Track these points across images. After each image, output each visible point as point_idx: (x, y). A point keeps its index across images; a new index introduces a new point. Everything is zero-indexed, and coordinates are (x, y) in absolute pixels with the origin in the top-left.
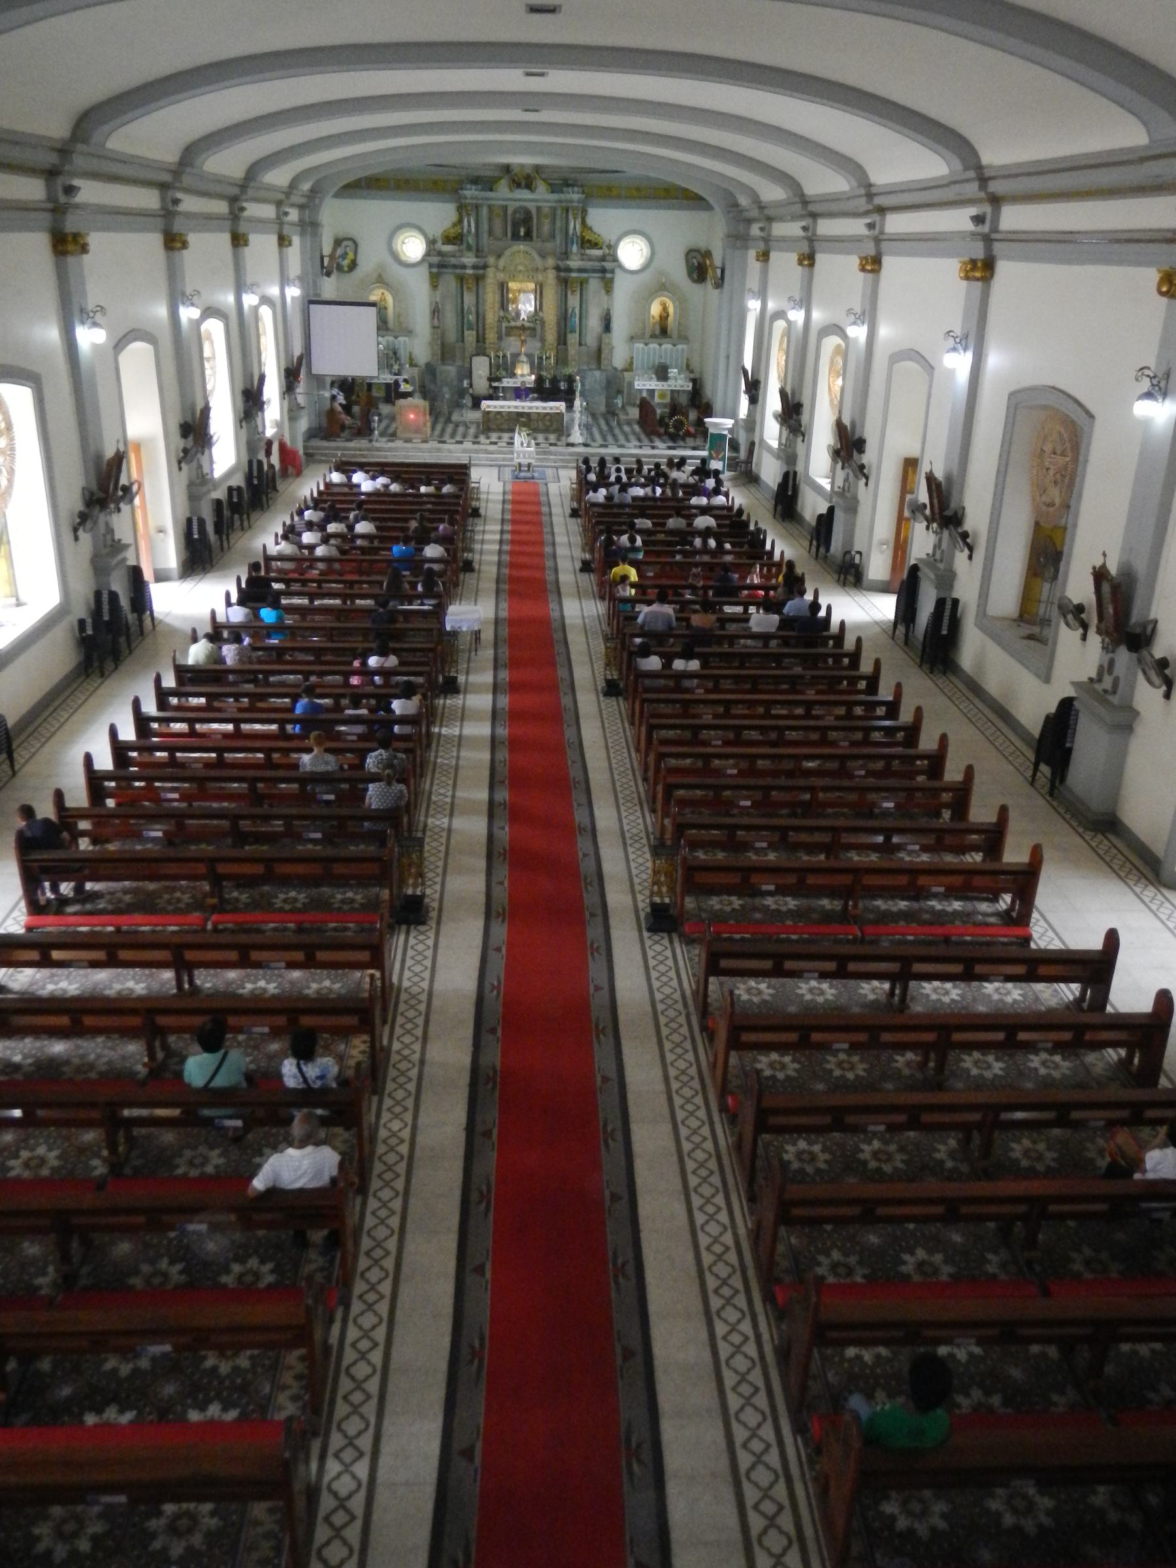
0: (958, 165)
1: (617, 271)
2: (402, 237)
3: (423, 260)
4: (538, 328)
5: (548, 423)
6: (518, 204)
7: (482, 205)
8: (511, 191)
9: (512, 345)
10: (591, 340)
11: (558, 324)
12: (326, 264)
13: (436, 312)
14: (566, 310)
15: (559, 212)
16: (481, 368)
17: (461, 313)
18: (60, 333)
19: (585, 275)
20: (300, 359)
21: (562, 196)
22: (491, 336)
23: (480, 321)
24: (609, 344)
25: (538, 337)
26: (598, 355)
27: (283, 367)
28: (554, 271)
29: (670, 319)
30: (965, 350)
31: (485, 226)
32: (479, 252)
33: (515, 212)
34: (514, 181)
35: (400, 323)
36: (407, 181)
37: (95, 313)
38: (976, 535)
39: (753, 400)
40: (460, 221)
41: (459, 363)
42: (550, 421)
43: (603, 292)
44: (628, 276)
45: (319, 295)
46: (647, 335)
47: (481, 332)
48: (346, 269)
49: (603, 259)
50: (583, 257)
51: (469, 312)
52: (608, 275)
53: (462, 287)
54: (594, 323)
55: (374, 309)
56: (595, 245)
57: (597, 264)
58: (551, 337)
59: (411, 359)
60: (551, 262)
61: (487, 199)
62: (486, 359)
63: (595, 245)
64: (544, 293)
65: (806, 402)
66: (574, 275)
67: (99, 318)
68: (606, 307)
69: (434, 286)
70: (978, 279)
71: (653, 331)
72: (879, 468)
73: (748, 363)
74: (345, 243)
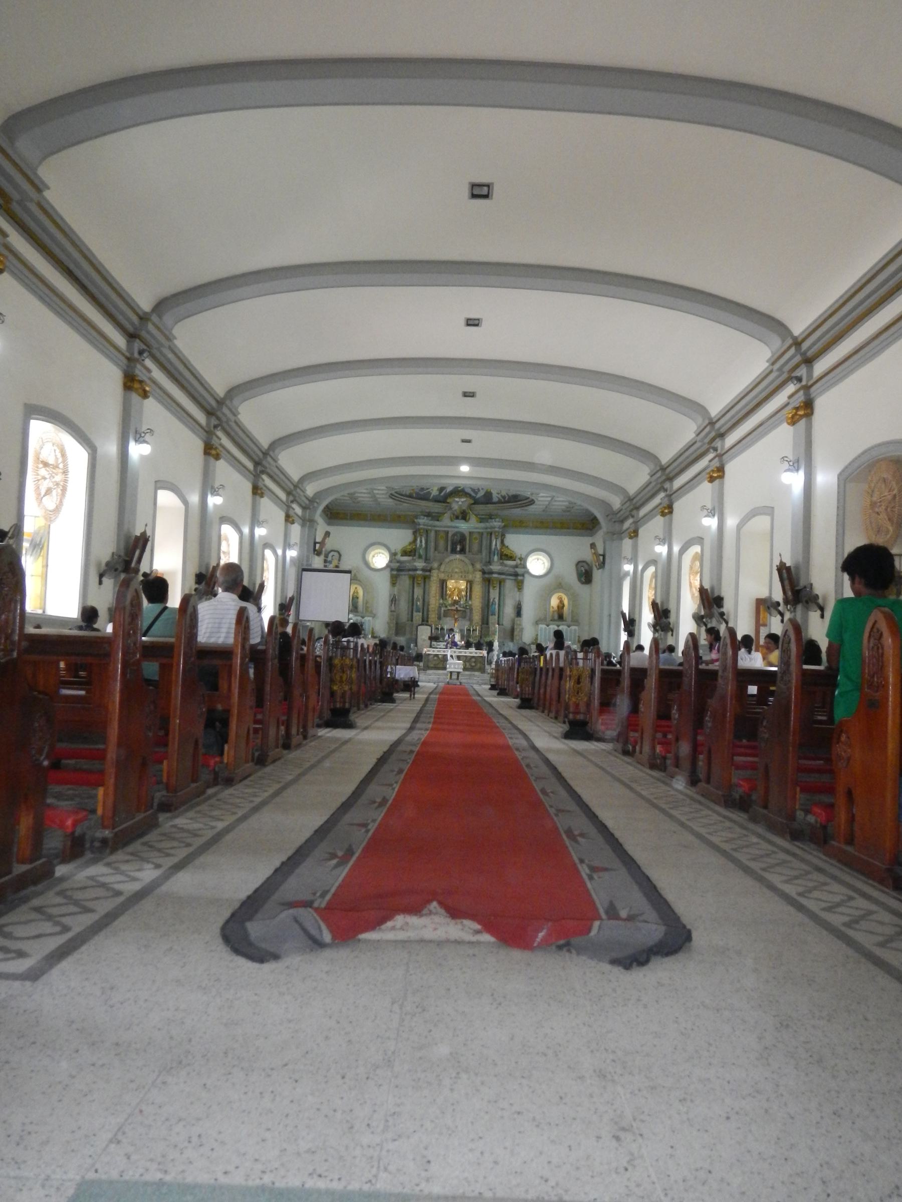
0: (777, 343)
1: (526, 576)
2: (373, 553)
3: (388, 566)
4: (468, 611)
6: (456, 530)
7: (431, 530)
8: (452, 520)
9: (447, 623)
10: (507, 622)
11: (483, 610)
12: (317, 548)
13: (393, 600)
14: (489, 600)
15: (485, 535)
16: (424, 632)
17: (412, 601)
18: (118, 449)
19: (503, 577)
20: (292, 599)
21: (487, 524)
22: (433, 616)
23: (426, 604)
24: (520, 625)
25: (467, 618)
26: (511, 634)
27: (279, 602)
28: (480, 573)
29: (566, 608)
30: (797, 470)
31: (432, 544)
32: (427, 560)
33: (454, 535)
35: (367, 608)
36: (379, 516)
37: (145, 434)
38: (825, 599)
39: (631, 634)
40: (415, 540)
41: (408, 636)
42: (475, 662)
43: (516, 589)
45: (311, 565)
46: (548, 619)
47: (425, 613)
49: (516, 566)
50: (502, 564)
51: (418, 600)
52: (520, 578)
53: (413, 584)
54: (509, 611)
55: (348, 575)
56: (511, 558)
57: (512, 570)
58: (477, 617)
59: (373, 633)
60: (478, 566)
61: (435, 526)
62: (429, 628)
63: (511, 558)
64: (473, 588)
65: (672, 607)
66: (495, 575)
67: (148, 437)
68: (518, 599)
69: (393, 583)
70: (802, 417)
71: (553, 616)
72: (736, 617)
73: (626, 609)
74: (332, 553)
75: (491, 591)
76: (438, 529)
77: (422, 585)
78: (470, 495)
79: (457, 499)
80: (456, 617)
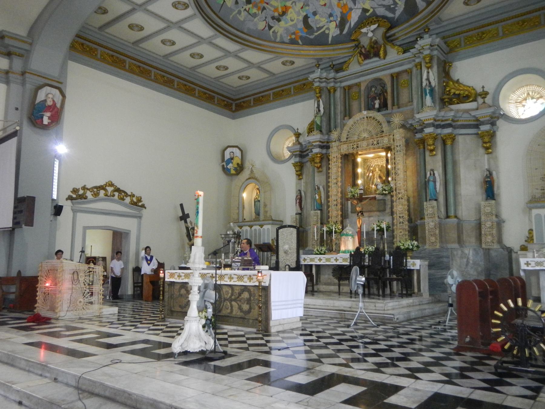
1: (500, 123)
5: (246, 307)
8: (361, 66)
15: (414, 70)
19: (448, 131)
25: (388, 210)
31: (340, 108)
34: (361, 53)
35: (266, 212)
42: (249, 301)
43: (482, 151)
44: (515, 126)
48: (233, 172)
52: (485, 128)
69: (300, 175)
74: (229, 150)
75: (428, 158)
76: (344, 84)
77: (324, 169)
78: (384, 17)
79: (364, 30)
80: (358, 209)
